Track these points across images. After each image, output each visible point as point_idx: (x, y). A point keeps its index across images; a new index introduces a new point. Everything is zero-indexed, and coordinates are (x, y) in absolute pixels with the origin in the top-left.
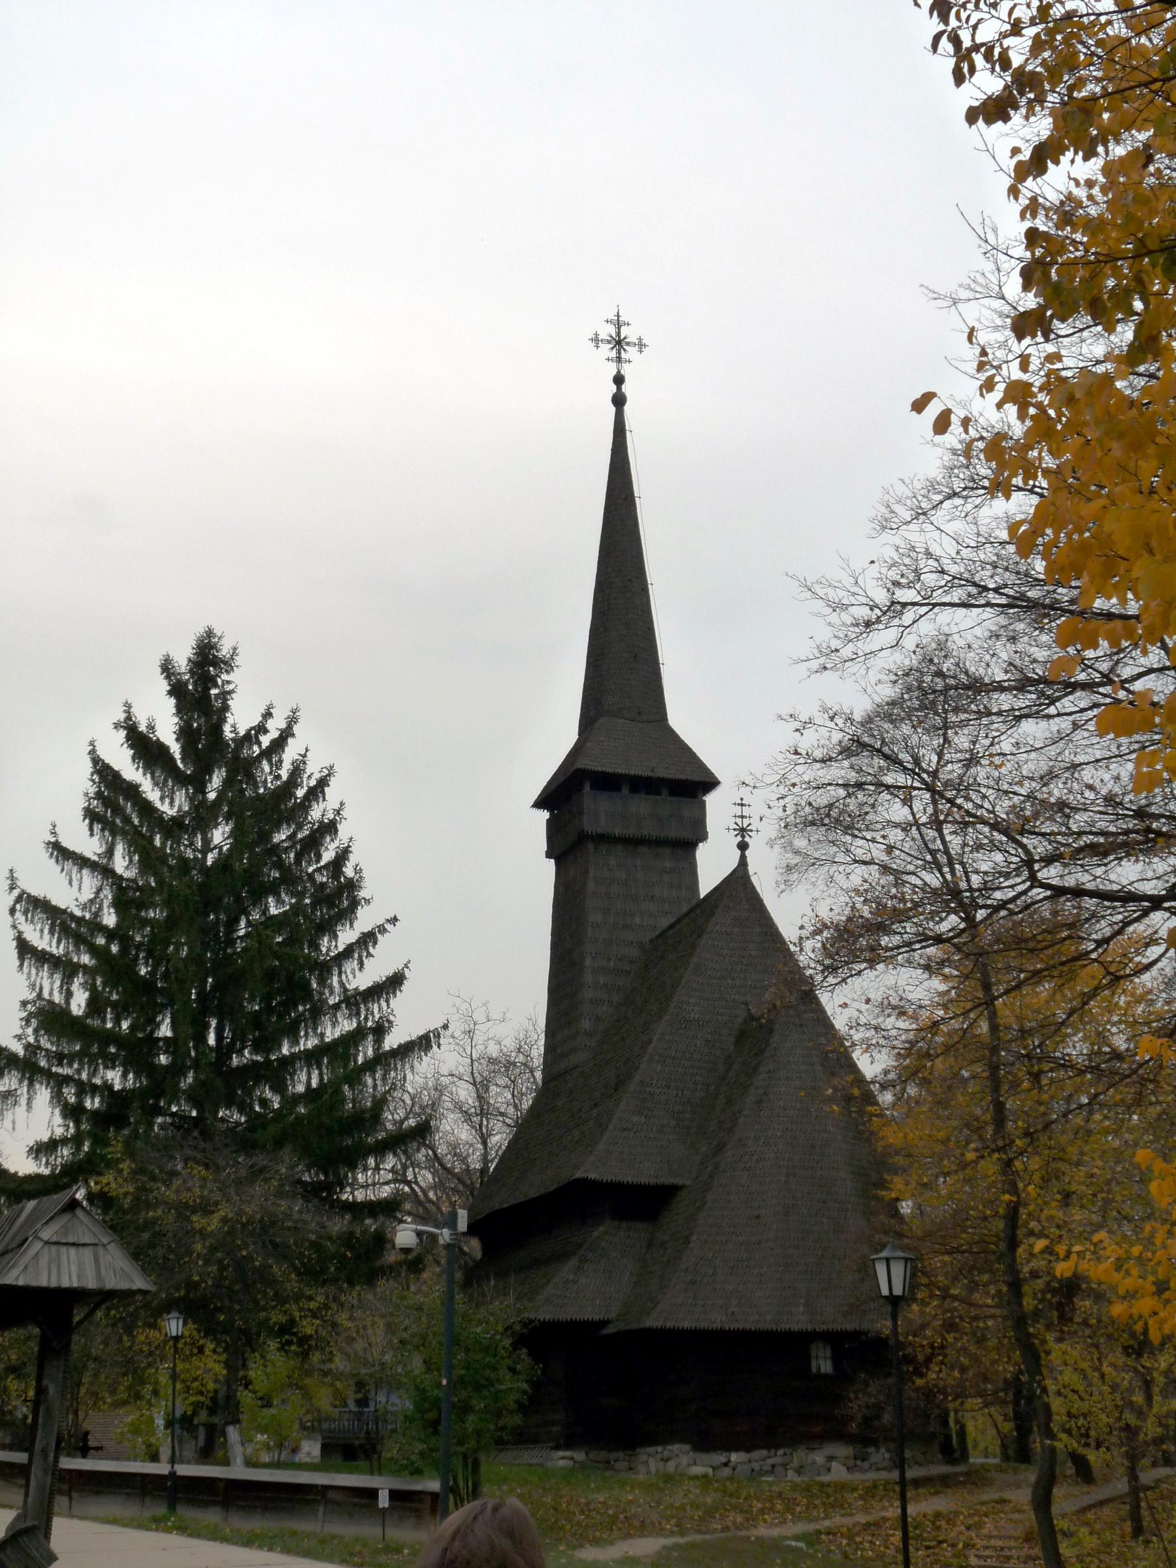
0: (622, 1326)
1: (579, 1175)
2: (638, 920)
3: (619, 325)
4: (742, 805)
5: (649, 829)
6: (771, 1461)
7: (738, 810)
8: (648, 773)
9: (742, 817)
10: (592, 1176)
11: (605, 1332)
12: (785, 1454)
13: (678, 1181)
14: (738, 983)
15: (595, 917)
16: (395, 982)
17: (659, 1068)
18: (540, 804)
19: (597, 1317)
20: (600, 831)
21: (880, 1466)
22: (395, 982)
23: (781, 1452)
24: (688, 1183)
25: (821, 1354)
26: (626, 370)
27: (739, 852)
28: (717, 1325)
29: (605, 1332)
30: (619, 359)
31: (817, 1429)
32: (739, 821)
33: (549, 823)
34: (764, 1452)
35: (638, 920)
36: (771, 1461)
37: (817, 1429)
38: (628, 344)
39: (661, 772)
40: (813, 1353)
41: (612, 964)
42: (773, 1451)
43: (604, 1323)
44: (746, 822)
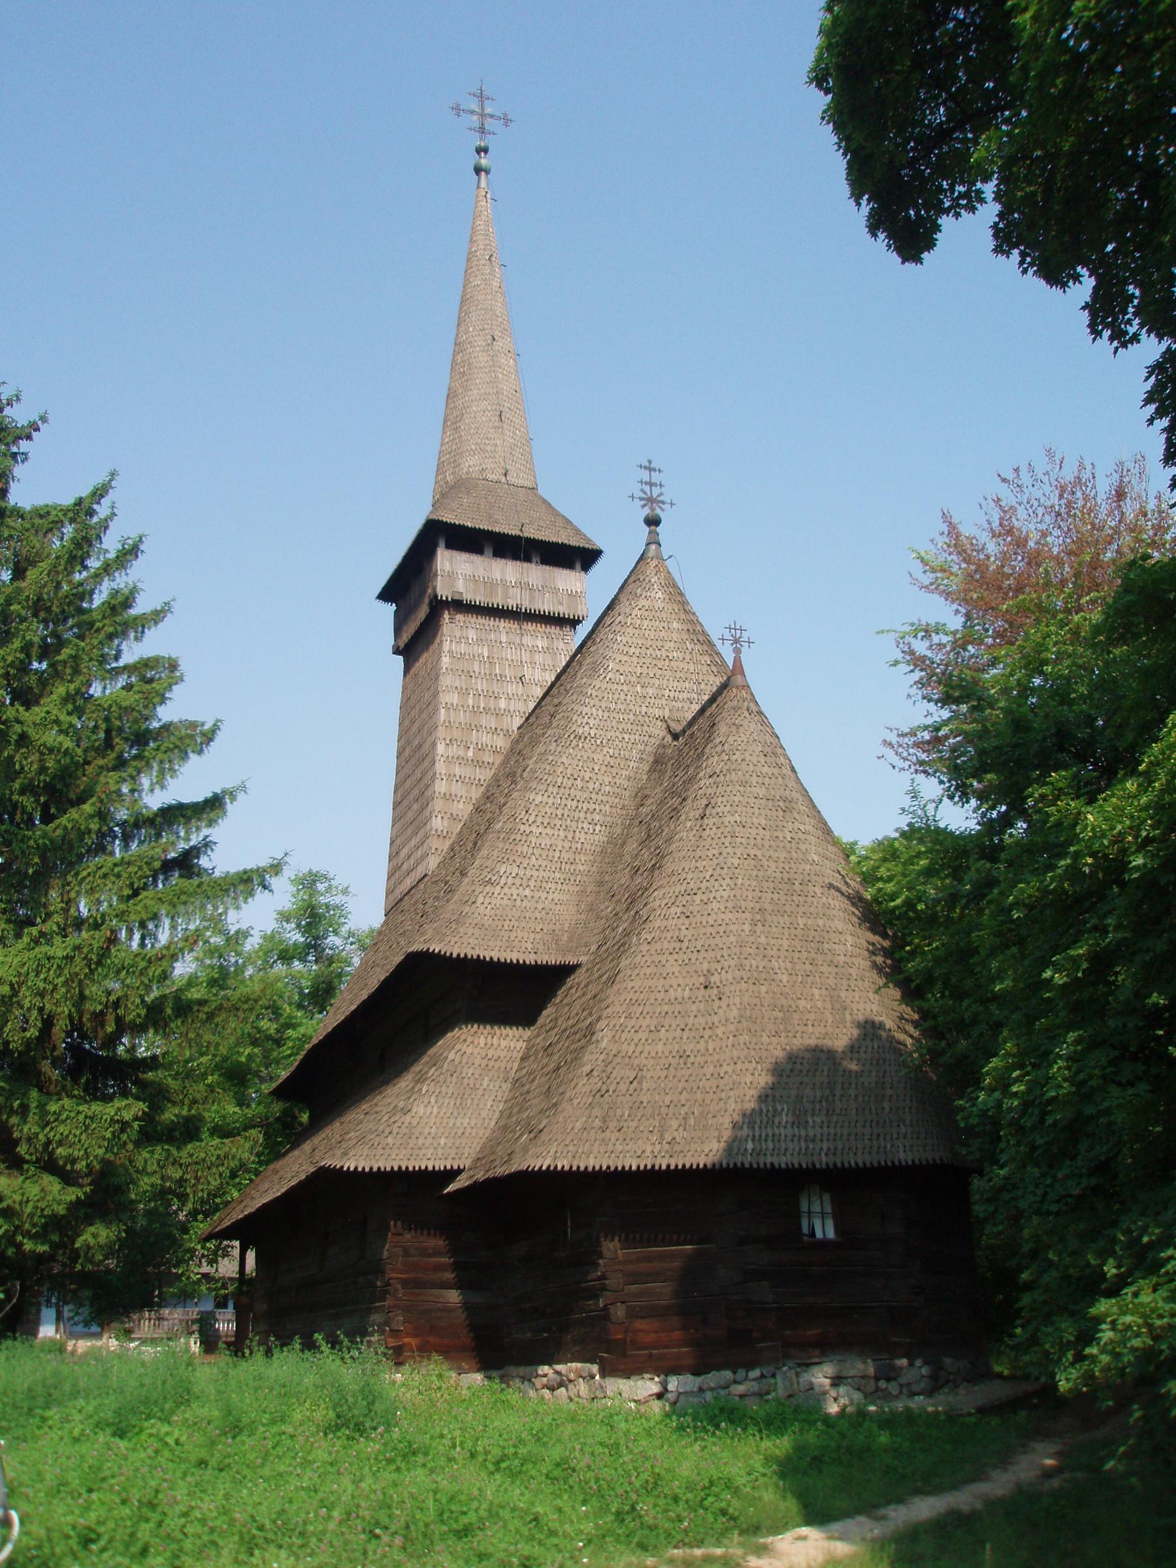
0: (480, 1176)
2: (503, 704)
3: (481, 97)
4: (651, 469)
5: (513, 601)
6: (741, 1389)
7: (645, 475)
8: (515, 532)
9: (651, 484)
10: (435, 947)
11: (451, 1188)
12: (763, 1376)
13: (571, 959)
14: (651, 691)
15: (453, 698)
16: (213, 806)
17: (539, 799)
19: (440, 1165)
20: (457, 597)
21: (916, 1388)
22: (213, 806)
23: (755, 1373)
24: (583, 959)
25: (816, 1207)
26: (489, 141)
27: (646, 529)
28: (646, 1162)
29: (451, 1188)
30: (482, 130)
31: (813, 1332)
32: (647, 489)
33: (396, 613)
34: (727, 1374)
35: (503, 704)
36: (741, 1389)
37: (813, 1332)
39: (531, 532)
40: (804, 1207)
41: (470, 754)
42: (741, 1373)
43: (452, 1174)
44: (656, 491)
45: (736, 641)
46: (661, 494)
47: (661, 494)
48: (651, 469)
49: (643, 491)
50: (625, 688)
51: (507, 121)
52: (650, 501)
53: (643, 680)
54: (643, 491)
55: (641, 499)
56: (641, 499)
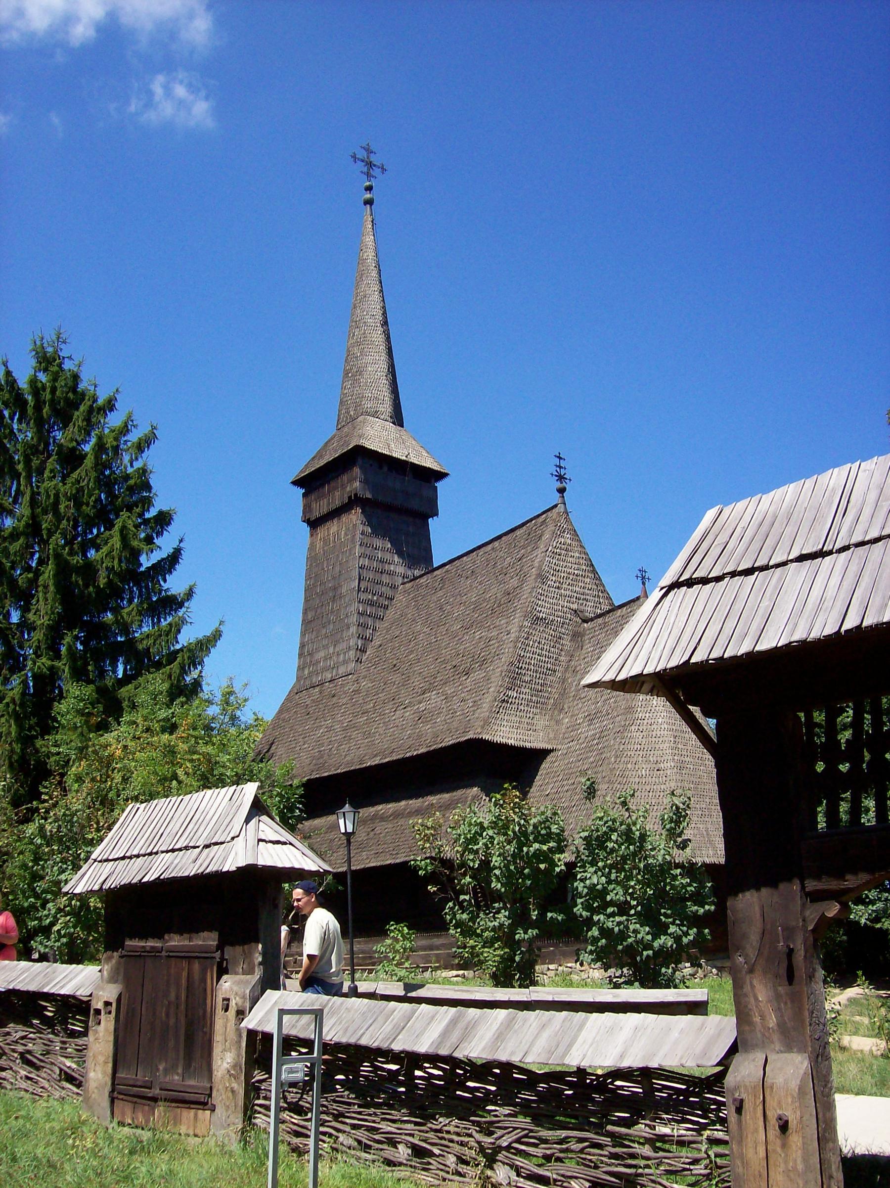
1: (470, 735)
3: (369, 151)
4: (560, 458)
8: (404, 458)
9: (560, 467)
10: (486, 737)
18: (296, 483)
26: (373, 183)
30: (369, 175)
32: (558, 469)
38: (375, 166)
41: (375, 598)
45: (643, 578)
46: (565, 474)
47: (565, 474)
48: (560, 458)
49: (557, 471)
50: (557, 590)
51: (383, 170)
52: (561, 478)
53: (564, 586)
54: (557, 471)
55: (556, 476)
56: (556, 476)
